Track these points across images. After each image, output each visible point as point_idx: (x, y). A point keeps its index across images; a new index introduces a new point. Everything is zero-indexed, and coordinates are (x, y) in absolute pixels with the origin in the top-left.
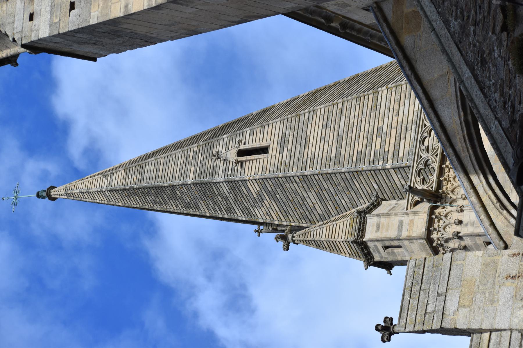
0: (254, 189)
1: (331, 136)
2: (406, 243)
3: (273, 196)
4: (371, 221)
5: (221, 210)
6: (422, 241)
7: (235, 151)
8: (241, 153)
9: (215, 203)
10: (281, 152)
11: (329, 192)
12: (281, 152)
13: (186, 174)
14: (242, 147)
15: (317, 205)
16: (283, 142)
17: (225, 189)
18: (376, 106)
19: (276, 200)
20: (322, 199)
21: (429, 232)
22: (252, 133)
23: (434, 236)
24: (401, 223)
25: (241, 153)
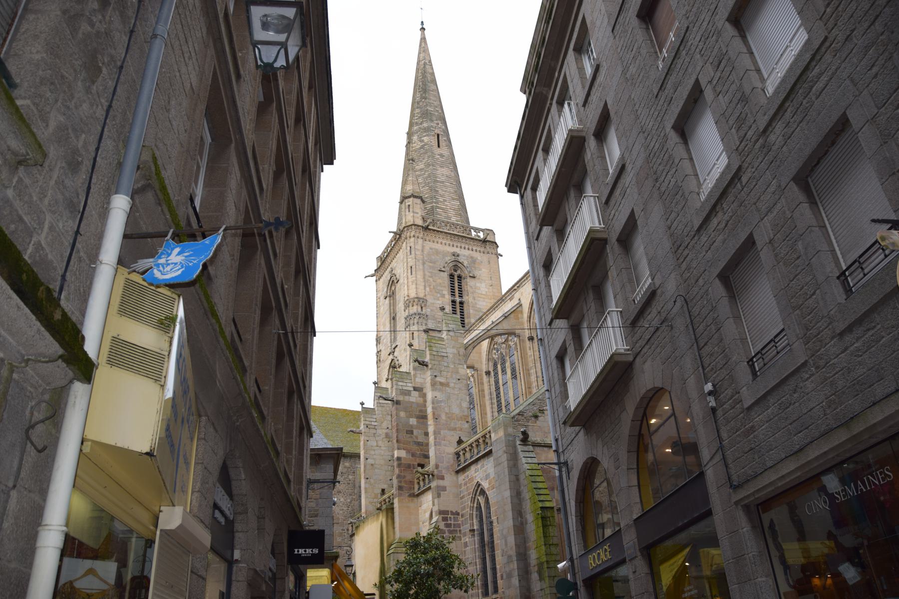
1: (443, 179)
2: (412, 214)
3: (422, 147)
4: (419, 201)
5: (417, 119)
6: (412, 221)
7: (439, 132)
8: (438, 135)
9: (420, 117)
10: (439, 155)
11: (424, 174)
12: (439, 155)
13: (431, 106)
14: (440, 136)
15: (571, 497)
16: (442, 156)
17: (425, 125)
18: (453, 199)
20: (421, 170)
21: (415, 225)
22: (445, 140)
23: (413, 227)
24: (417, 213)
25: (438, 135)
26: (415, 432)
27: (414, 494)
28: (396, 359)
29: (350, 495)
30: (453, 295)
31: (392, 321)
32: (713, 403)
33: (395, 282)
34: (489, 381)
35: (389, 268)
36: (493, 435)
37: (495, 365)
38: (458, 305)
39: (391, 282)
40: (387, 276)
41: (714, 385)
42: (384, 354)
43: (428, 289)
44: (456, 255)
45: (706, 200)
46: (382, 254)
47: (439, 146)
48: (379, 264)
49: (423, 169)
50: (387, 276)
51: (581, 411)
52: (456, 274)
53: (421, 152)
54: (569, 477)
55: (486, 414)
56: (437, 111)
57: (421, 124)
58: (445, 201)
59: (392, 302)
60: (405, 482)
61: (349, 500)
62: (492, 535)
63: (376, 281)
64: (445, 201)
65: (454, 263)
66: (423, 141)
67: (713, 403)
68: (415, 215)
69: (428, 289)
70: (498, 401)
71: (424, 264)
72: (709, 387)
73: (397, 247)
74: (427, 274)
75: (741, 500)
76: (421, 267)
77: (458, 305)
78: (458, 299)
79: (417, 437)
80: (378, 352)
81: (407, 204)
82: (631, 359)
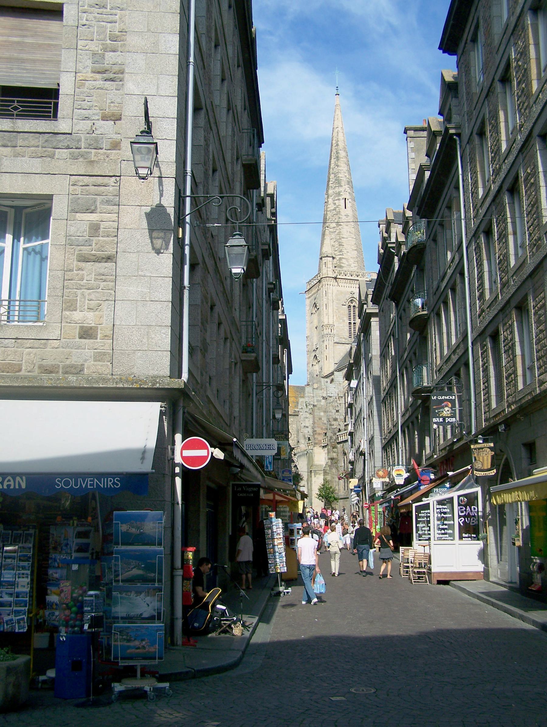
3: (335, 209)
10: (345, 215)
11: (335, 232)
12: (345, 215)
19: (334, 210)
43: (335, 318)
53: (334, 213)
56: (346, 176)
57: (334, 189)
58: (348, 252)
64: (348, 252)
66: (335, 204)
68: (329, 269)
69: (335, 318)
71: (333, 301)
74: (336, 308)
76: (332, 304)
78: (352, 322)
81: (324, 261)
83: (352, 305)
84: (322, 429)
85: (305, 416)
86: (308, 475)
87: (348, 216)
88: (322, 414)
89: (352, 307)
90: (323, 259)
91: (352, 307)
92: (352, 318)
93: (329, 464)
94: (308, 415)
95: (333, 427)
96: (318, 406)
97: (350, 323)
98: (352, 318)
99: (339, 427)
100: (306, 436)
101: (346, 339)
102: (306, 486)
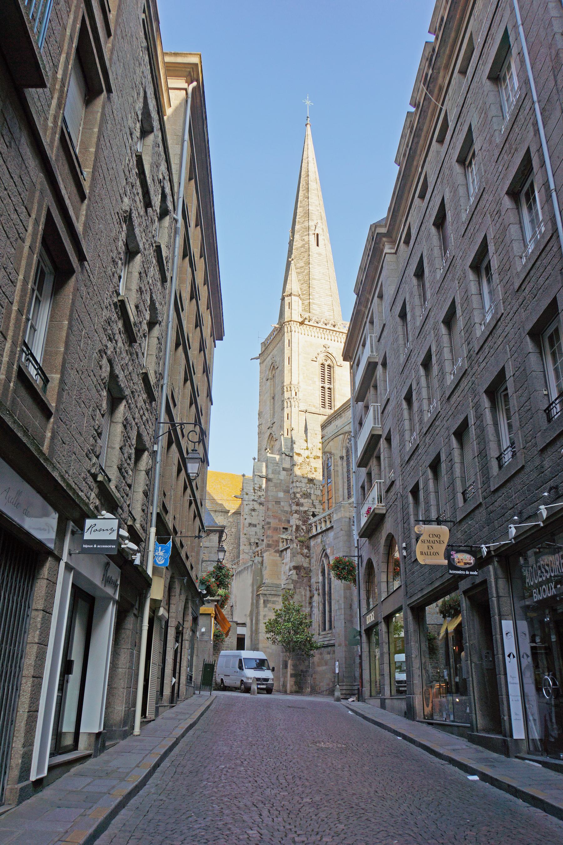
0: (306, 238)
3: (303, 246)
16: (320, 254)
19: (302, 247)
25: (317, 235)
26: (282, 504)
27: (278, 550)
28: (273, 433)
29: (232, 544)
30: (323, 381)
31: (272, 400)
32: (405, 554)
33: (276, 367)
34: (342, 465)
35: (271, 354)
36: (335, 515)
37: (348, 451)
38: (327, 390)
39: (272, 367)
40: (269, 361)
41: (406, 545)
42: (264, 428)
44: (327, 347)
45: (409, 451)
46: (266, 340)
47: (318, 245)
48: (263, 349)
49: (303, 267)
50: (269, 361)
51: (366, 528)
52: (326, 364)
53: (302, 251)
54: (362, 565)
55: (338, 490)
56: (318, 210)
59: (272, 383)
60: (273, 541)
61: (231, 548)
62: (330, 588)
63: (260, 364)
65: (326, 354)
67: (405, 554)
70: (348, 481)
72: (404, 545)
73: (278, 339)
75: (410, 604)
77: (327, 390)
78: (327, 386)
79: (283, 507)
80: (259, 425)
82: (384, 512)
83: (326, 364)
84: (280, 520)
85: (251, 507)
86: (252, 604)
87: (321, 255)
88: (281, 495)
89: (326, 367)
90: (286, 298)
91: (326, 367)
92: (326, 381)
93: (295, 577)
94: (256, 506)
95: (301, 509)
96: (274, 481)
97: (322, 387)
98: (326, 381)
99: (313, 510)
100: (252, 540)
101: (317, 408)
102: (248, 624)
